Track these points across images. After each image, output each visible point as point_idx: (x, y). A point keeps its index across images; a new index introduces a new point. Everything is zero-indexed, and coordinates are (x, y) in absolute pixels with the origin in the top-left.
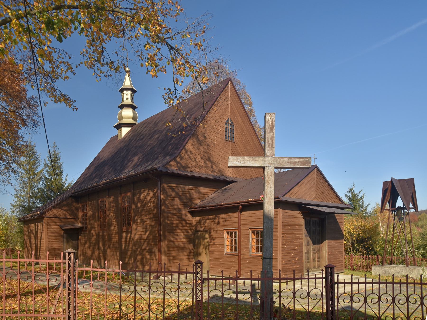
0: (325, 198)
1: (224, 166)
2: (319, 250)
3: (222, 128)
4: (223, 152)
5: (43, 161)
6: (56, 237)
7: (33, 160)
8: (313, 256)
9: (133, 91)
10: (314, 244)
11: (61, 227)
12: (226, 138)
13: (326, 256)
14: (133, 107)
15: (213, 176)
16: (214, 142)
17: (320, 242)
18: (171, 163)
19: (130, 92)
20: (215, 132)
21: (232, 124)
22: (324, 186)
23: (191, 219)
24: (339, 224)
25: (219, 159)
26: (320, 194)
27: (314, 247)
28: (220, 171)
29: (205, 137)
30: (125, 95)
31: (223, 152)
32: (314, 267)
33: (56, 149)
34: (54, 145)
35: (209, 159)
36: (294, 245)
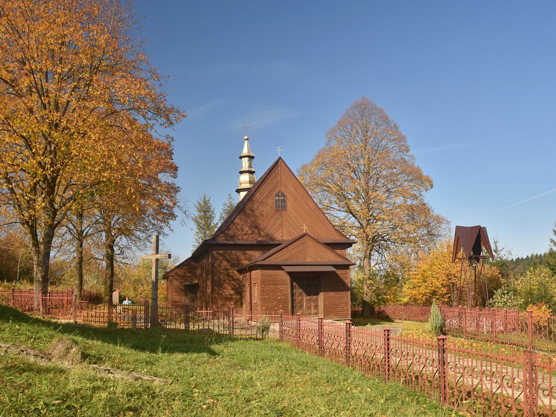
0: (319, 258)
1: (274, 232)
2: (316, 299)
3: (271, 201)
4: (273, 220)
5: (219, 214)
6: (177, 292)
7: (208, 214)
8: (307, 304)
9: (251, 158)
10: (308, 294)
11: (181, 283)
12: (276, 208)
13: (321, 305)
14: (251, 173)
15: (259, 241)
16: (263, 214)
17: (317, 294)
18: (220, 235)
19: (247, 158)
20: (264, 206)
21: (283, 195)
22: (319, 249)
23: (238, 276)
24: (342, 278)
25: (268, 226)
26: (312, 255)
27: (308, 298)
28: (267, 235)
29: (253, 211)
30: (243, 162)
31: (273, 220)
32: (310, 314)
33: (231, 200)
34: (229, 197)
35: (256, 227)
36: (276, 296)
